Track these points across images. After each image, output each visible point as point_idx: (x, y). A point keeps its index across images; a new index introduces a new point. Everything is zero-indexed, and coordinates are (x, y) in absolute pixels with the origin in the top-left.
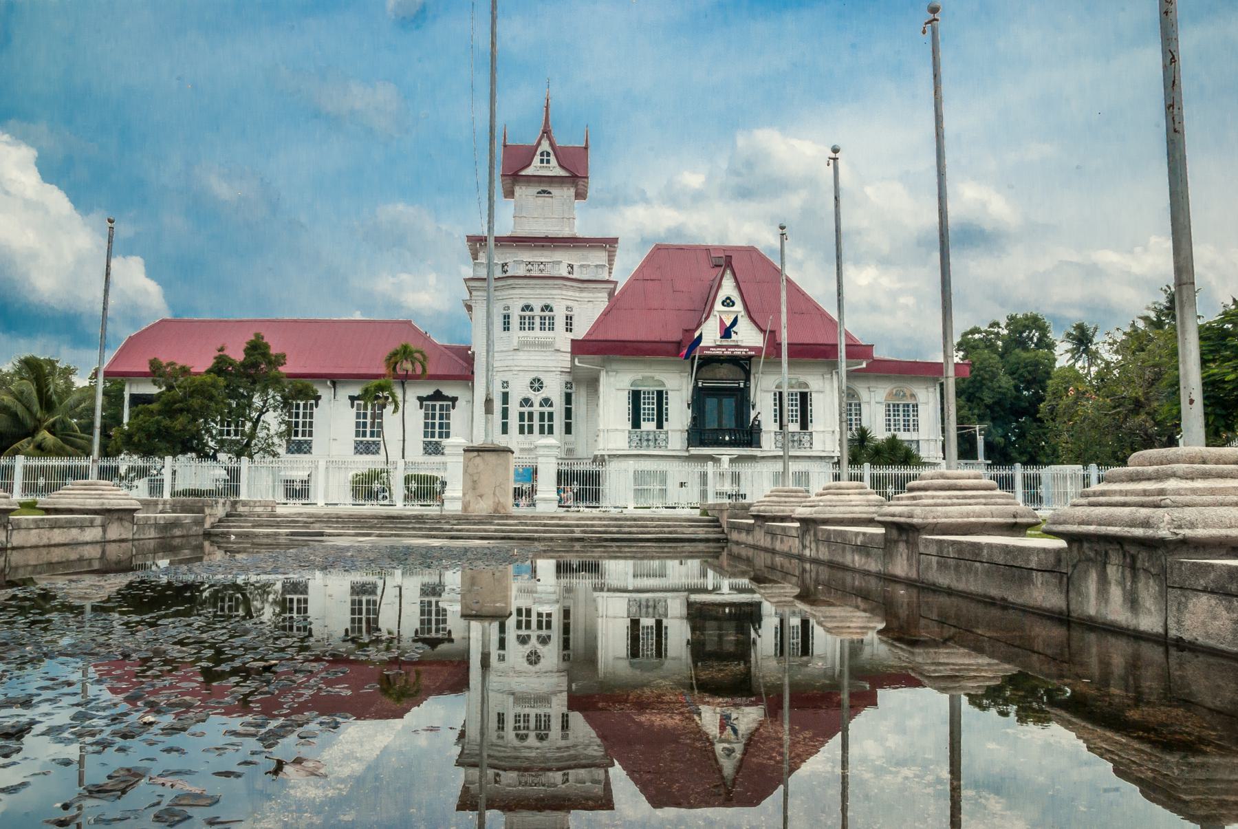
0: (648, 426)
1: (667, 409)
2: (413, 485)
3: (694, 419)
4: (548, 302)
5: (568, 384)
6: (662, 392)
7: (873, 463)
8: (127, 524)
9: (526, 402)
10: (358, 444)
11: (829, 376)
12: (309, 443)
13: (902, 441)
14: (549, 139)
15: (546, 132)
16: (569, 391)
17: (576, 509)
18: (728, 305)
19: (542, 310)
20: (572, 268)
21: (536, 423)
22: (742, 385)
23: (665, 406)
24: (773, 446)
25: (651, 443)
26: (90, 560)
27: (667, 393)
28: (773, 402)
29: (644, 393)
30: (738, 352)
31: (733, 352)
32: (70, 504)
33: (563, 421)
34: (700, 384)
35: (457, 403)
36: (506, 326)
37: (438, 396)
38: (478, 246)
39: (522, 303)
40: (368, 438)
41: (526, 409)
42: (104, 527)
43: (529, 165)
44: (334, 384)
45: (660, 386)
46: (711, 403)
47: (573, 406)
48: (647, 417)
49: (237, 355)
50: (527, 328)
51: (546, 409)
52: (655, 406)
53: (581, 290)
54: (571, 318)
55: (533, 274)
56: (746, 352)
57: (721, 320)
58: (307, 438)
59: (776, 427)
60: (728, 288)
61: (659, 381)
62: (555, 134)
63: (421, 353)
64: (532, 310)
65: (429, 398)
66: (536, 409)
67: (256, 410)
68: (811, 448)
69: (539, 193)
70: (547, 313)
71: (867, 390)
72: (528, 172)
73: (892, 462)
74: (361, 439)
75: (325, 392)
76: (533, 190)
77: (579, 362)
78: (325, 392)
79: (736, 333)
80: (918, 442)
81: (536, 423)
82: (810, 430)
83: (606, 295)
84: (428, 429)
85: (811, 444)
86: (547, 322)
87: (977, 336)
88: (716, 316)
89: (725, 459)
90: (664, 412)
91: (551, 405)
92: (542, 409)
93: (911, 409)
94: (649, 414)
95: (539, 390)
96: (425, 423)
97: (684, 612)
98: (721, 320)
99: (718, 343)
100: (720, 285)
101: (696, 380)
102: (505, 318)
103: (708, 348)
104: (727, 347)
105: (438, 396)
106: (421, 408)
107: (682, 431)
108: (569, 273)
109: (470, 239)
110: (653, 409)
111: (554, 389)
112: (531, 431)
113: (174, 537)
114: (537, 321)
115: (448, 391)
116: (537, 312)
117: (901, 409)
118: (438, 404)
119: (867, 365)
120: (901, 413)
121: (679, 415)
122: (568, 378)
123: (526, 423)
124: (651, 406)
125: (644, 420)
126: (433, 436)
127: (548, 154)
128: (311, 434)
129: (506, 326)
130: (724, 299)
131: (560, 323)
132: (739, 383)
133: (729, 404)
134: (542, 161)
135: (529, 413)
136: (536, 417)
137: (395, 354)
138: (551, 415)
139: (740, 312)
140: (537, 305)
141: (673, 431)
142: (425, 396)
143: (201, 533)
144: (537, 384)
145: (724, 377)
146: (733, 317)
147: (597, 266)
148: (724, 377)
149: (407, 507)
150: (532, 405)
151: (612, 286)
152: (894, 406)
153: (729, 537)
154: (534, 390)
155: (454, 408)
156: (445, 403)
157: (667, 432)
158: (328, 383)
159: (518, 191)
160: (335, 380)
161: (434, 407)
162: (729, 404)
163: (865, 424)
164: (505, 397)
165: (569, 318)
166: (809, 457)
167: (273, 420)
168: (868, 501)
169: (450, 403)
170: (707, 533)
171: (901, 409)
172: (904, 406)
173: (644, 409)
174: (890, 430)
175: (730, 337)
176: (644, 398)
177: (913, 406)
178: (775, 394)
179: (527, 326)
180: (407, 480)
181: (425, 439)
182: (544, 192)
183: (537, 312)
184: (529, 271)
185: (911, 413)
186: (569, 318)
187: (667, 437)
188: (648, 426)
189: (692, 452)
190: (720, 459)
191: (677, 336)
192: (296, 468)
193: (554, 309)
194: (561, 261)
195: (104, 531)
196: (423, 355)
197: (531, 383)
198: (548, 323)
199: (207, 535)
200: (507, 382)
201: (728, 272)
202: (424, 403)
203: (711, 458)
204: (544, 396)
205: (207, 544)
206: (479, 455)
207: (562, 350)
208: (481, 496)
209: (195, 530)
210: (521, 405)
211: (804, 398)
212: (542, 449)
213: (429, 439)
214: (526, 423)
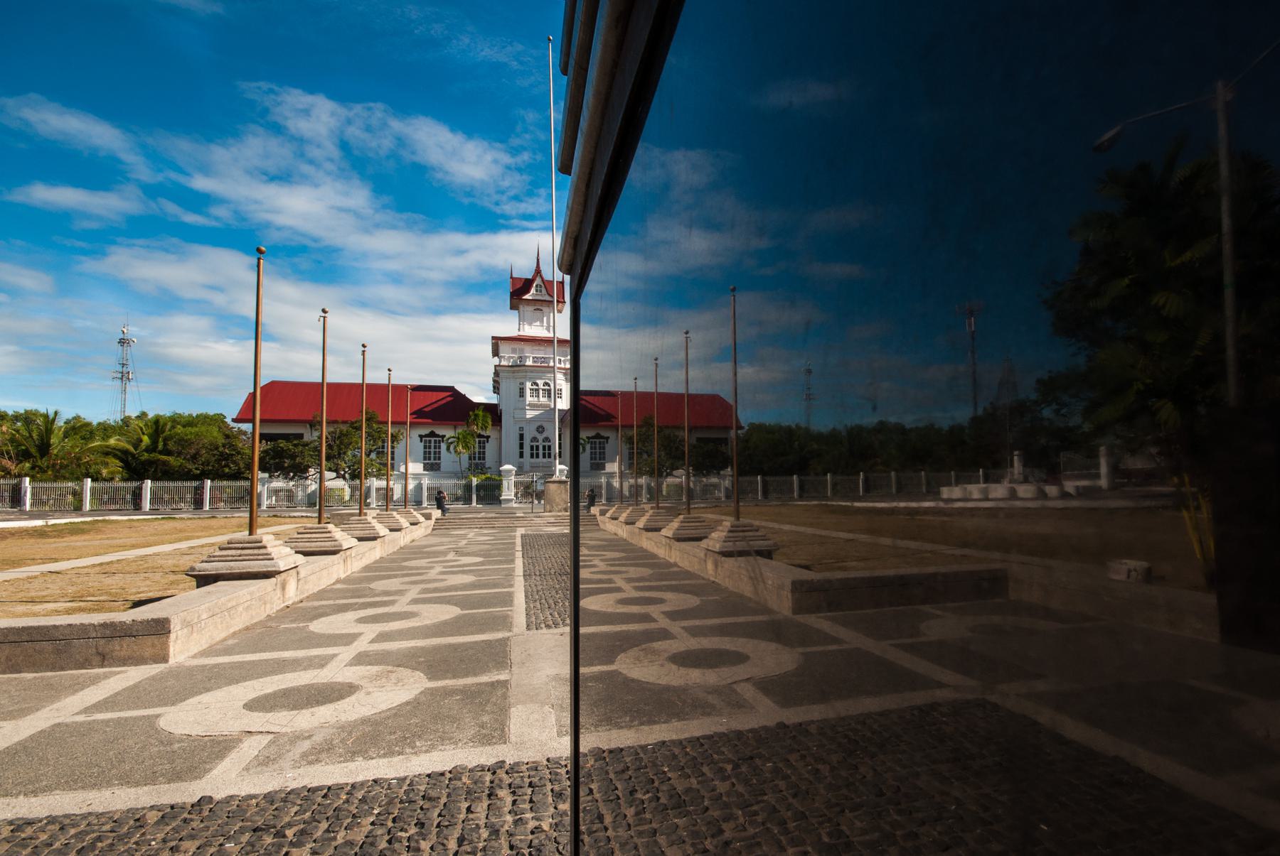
9: (534, 439)
14: (541, 276)
15: (538, 271)
21: (541, 452)
35: (489, 439)
40: (432, 461)
43: (528, 291)
51: (547, 444)
74: (427, 461)
81: (541, 452)
92: (544, 444)
102: (520, 389)
109: (493, 338)
112: (537, 457)
114: (541, 392)
123: (535, 452)
127: (541, 286)
134: (537, 291)
136: (541, 448)
150: (538, 441)
155: (488, 442)
164: (521, 437)
169: (485, 439)
182: (538, 309)
200: (523, 428)
210: (532, 441)
214: (535, 452)
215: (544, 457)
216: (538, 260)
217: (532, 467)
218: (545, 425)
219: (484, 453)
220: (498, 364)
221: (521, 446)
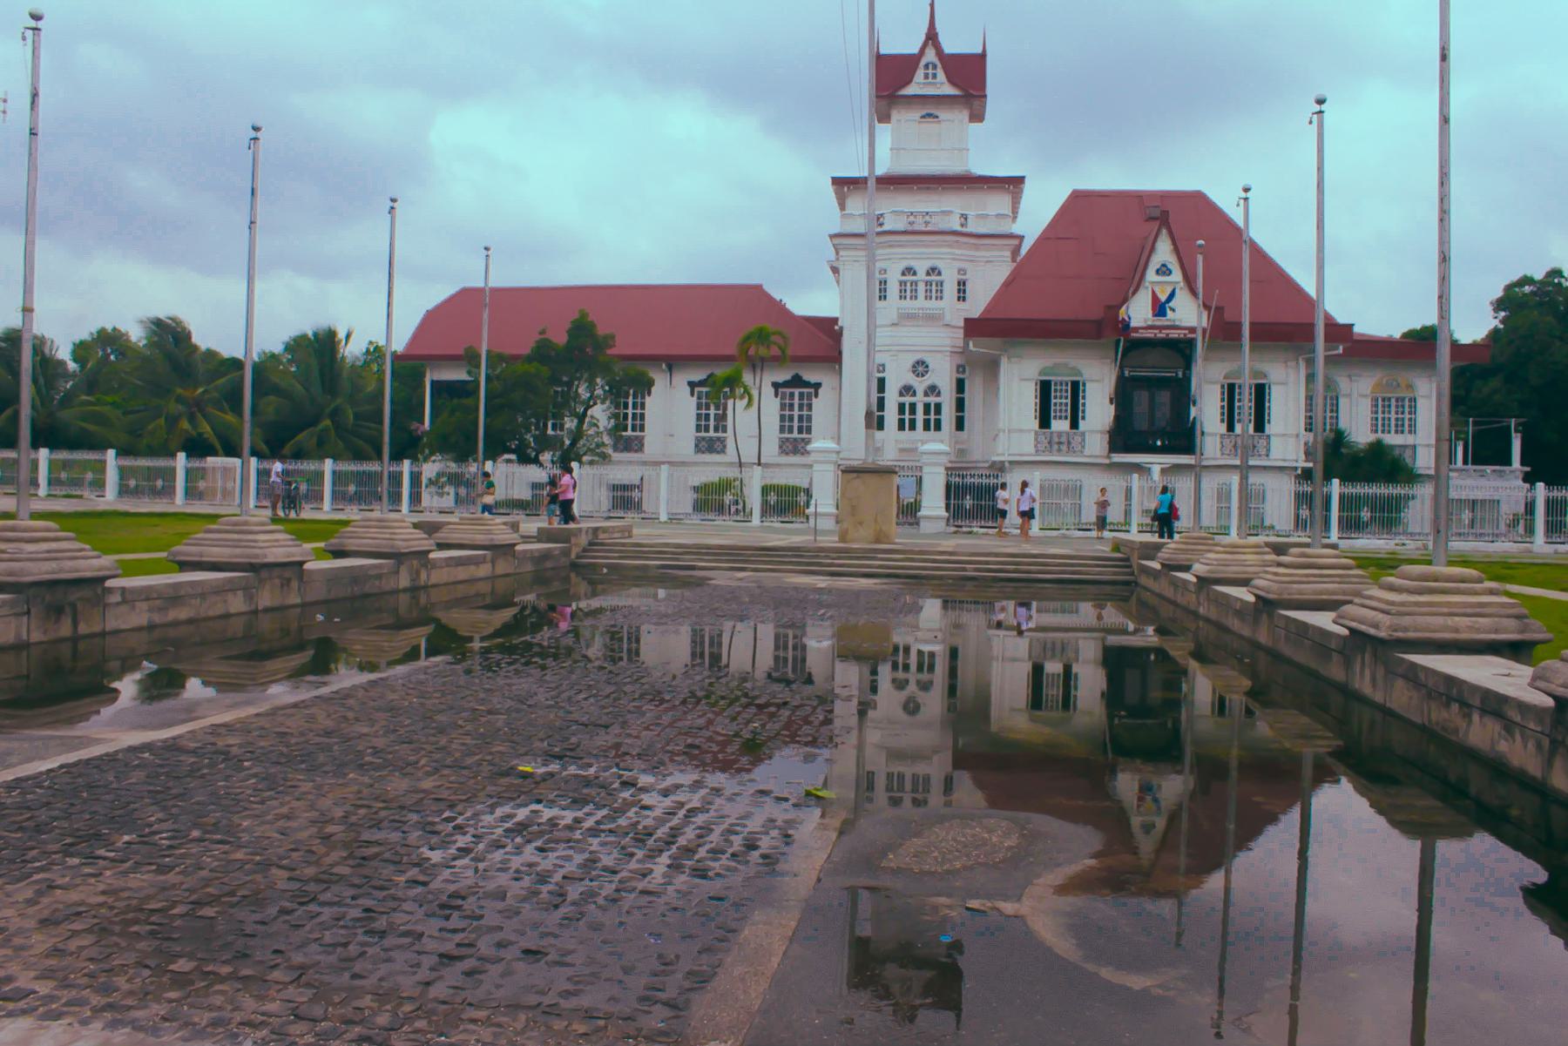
0: (1060, 425)
1: (1084, 405)
2: (773, 498)
3: (1117, 418)
4: (939, 264)
5: (960, 368)
7: (1344, 479)
8: (510, 558)
9: (907, 390)
10: (698, 441)
12: (641, 441)
13: (1392, 447)
15: (932, 37)
16: (961, 376)
17: (969, 529)
18: (1164, 274)
19: (928, 274)
20: (966, 219)
21: (920, 416)
22: (1180, 375)
23: (1081, 401)
24: (1218, 454)
25: (1064, 447)
26: (484, 595)
27: (1084, 385)
28: (1219, 396)
29: (1056, 384)
30: (1174, 334)
31: (1167, 335)
32: (461, 539)
33: (954, 414)
34: (1126, 373)
36: (883, 294)
37: (797, 381)
38: (846, 189)
39: (905, 264)
41: (907, 400)
42: (493, 562)
43: (909, 82)
44: (670, 368)
45: (1076, 375)
46: (1141, 399)
47: (966, 395)
48: (1058, 414)
49: (560, 338)
50: (908, 297)
51: (932, 400)
52: (1069, 401)
53: (977, 247)
54: (964, 284)
55: (917, 227)
56: (1185, 335)
57: (1153, 292)
58: (638, 433)
59: (1223, 428)
60: (1164, 252)
61: (1073, 368)
62: (942, 39)
63: (780, 334)
64: (915, 274)
65: (786, 384)
66: (920, 399)
67: (582, 403)
68: (1267, 456)
69: (923, 117)
70: (934, 278)
71: (1348, 380)
72: (910, 90)
73: (1369, 479)
75: (660, 380)
76: (916, 114)
77: (974, 346)
78: (660, 380)
79: (1173, 310)
80: (1414, 447)
81: (920, 416)
82: (1267, 431)
83: (1008, 254)
84: (785, 423)
85: (1268, 450)
86: (934, 287)
87: (1527, 289)
88: (1147, 288)
89: (1156, 469)
90: (1081, 408)
91: (939, 394)
92: (928, 400)
93: (1407, 403)
94: (1061, 411)
95: (923, 376)
96: (781, 416)
97: (1100, 654)
98: (1153, 292)
99: (1150, 323)
100: (1153, 249)
101: (1121, 368)
103: (1136, 329)
104: (1161, 328)
105: (797, 381)
106: (776, 395)
107: (1102, 432)
108: (962, 225)
110: (1066, 404)
111: (943, 374)
112: (913, 427)
113: (546, 570)
114: (921, 287)
116: (921, 275)
117: (1393, 402)
118: (797, 392)
119: (1344, 350)
120: (1393, 409)
121: (1099, 411)
122: (959, 360)
123: (907, 417)
124: (1064, 401)
125: (1055, 417)
126: (791, 431)
128: (642, 428)
129: (883, 294)
130: (1158, 266)
131: (950, 289)
133: (1164, 397)
134: (926, 77)
135: (910, 404)
136: (920, 409)
137: (748, 337)
138: (938, 407)
140: (921, 267)
141: (1092, 432)
142: (781, 381)
143: (568, 563)
144: (920, 368)
145: (1153, 366)
147: (998, 216)
149: (765, 524)
151: (1016, 242)
152: (1383, 400)
153: (1139, 581)
154: (918, 376)
155: (816, 396)
156: (805, 390)
157: (1083, 434)
158: (664, 366)
159: (895, 115)
160: (672, 363)
161: (792, 395)
162: (1164, 397)
163: (1342, 425)
165: (962, 285)
166: (1265, 468)
167: (600, 414)
168: (1264, 561)
169: (812, 390)
170: (1115, 574)
171: (1393, 402)
172: (1397, 400)
173: (1055, 404)
174: (1376, 431)
175: (1164, 315)
176: (1056, 391)
177: (1410, 400)
178: (1223, 387)
180: (766, 490)
181: (783, 436)
182: (929, 115)
183: (921, 275)
184: (911, 223)
185: (1407, 410)
186: (962, 285)
187: (1084, 440)
190: (1149, 469)
191: (1096, 313)
192: (623, 470)
193: (943, 273)
194: (949, 209)
195: (493, 567)
196: (784, 337)
197: (914, 366)
198: (935, 289)
199: (574, 566)
200: (883, 365)
201: (1164, 231)
202: (780, 390)
203: (1138, 468)
205: (573, 575)
206: (858, 477)
207: (953, 323)
208: (861, 523)
209: (564, 561)
210: (901, 394)
211: (1261, 393)
213: (786, 435)
215: (927, 427)
217: (902, 450)
218: (928, 359)
220: (837, 230)
221: (881, 404)
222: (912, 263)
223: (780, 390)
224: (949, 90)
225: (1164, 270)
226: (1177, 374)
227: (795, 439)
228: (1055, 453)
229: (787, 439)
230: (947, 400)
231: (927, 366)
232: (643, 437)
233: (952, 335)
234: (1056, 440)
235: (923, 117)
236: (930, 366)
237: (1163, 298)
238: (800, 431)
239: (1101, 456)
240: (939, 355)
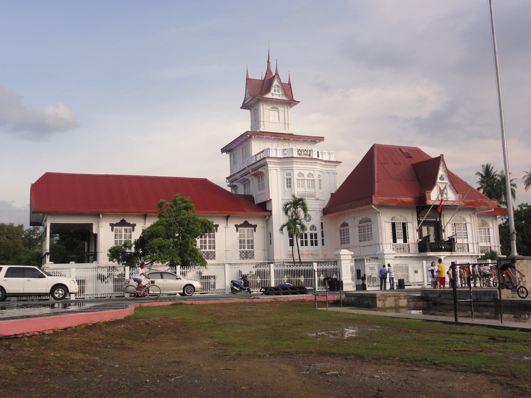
0: (400, 241)
4: (312, 172)
6: (405, 223)
11: (472, 215)
16: (322, 221)
21: (309, 239)
22: (438, 220)
35: (257, 228)
39: (299, 171)
40: (208, 250)
47: (324, 230)
51: (313, 232)
55: (287, 156)
56: (452, 204)
68: (468, 251)
69: (271, 108)
81: (309, 239)
91: (316, 230)
95: (309, 221)
102: (287, 180)
112: (306, 245)
115: (252, 222)
121: (413, 237)
125: (398, 238)
126: (244, 248)
132: (437, 219)
134: (275, 91)
138: (316, 235)
139: (448, 183)
140: (306, 173)
146: (444, 185)
148: (431, 216)
155: (255, 231)
179: (301, 185)
182: (274, 108)
188: (400, 241)
189: (428, 255)
204: (312, 224)
212: (388, 255)
215: (312, 244)
216: (268, 62)
219: (252, 241)
222: (302, 172)
223: (239, 228)
224: (284, 98)
225: (442, 178)
226: (437, 220)
227: (247, 251)
228: (407, 253)
229: (243, 251)
230: (318, 232)
231: (310, 217)
232: (215, 252)
233: (318, 203)
234: (399, 247)
235: (271, 108)
236: (312, 217)
237: (442, 189)
238: (248, 248)
239: (417, 254)
240: (316, 212)
